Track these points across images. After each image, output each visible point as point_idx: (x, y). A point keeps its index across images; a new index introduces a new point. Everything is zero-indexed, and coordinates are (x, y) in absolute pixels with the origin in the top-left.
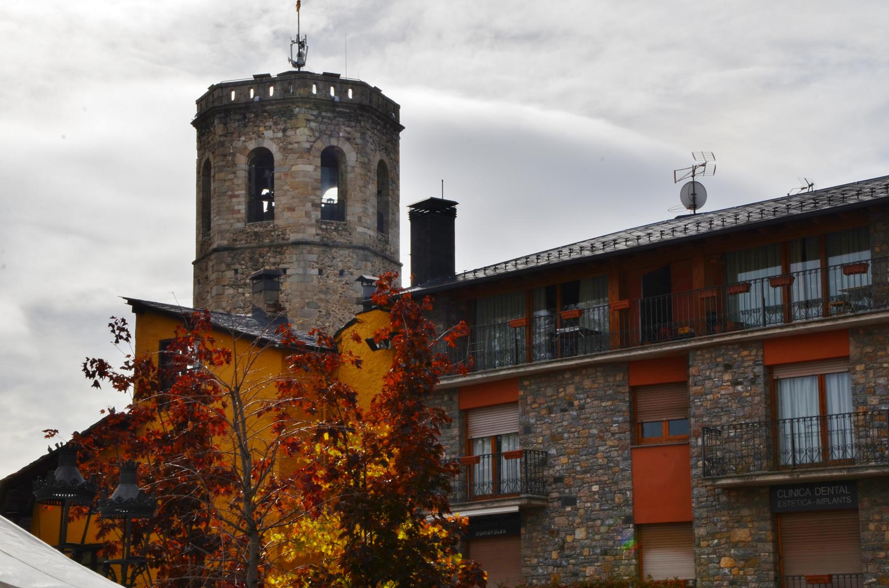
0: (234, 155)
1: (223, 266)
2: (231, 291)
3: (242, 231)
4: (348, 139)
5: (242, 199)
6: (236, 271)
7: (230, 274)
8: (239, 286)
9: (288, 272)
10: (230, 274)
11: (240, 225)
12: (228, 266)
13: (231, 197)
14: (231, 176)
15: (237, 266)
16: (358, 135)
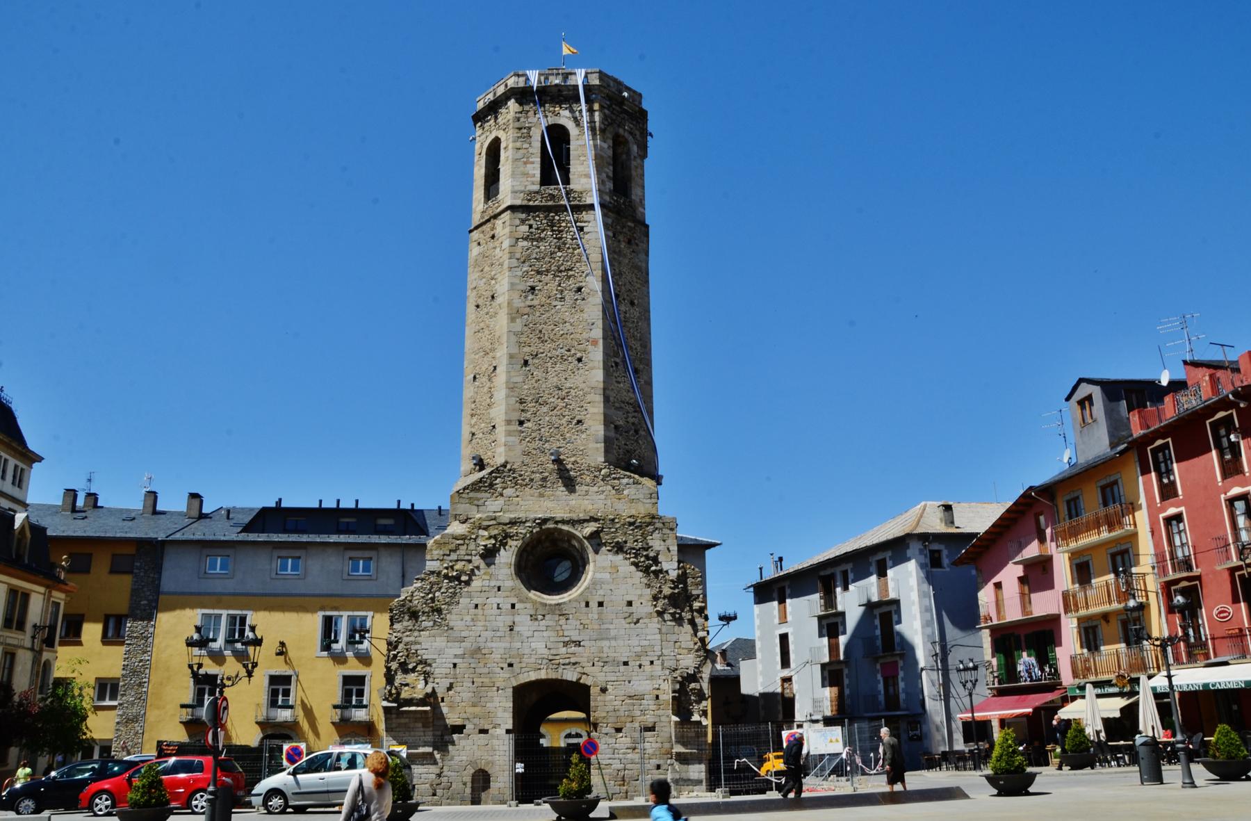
0: (530, 128)
1: (518, 222)
2: (525, 243)
3: (537, 193)
4: (631, 133)
5: (538, 166)
6: (531, 227)
7: (525, 228)
8: (533, 240)
9: (586, 230)
10: (525, 228)
11: (536, 187)
12: (523, 221)
13: (525, 163)
14: (526, 146)
15: (532, 222)
16: (638, 133)
